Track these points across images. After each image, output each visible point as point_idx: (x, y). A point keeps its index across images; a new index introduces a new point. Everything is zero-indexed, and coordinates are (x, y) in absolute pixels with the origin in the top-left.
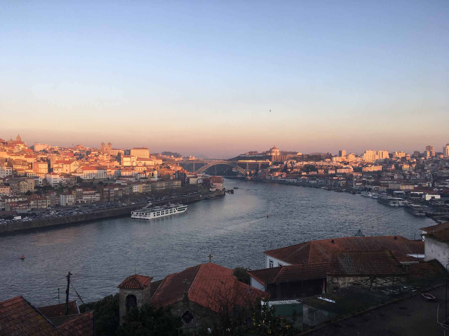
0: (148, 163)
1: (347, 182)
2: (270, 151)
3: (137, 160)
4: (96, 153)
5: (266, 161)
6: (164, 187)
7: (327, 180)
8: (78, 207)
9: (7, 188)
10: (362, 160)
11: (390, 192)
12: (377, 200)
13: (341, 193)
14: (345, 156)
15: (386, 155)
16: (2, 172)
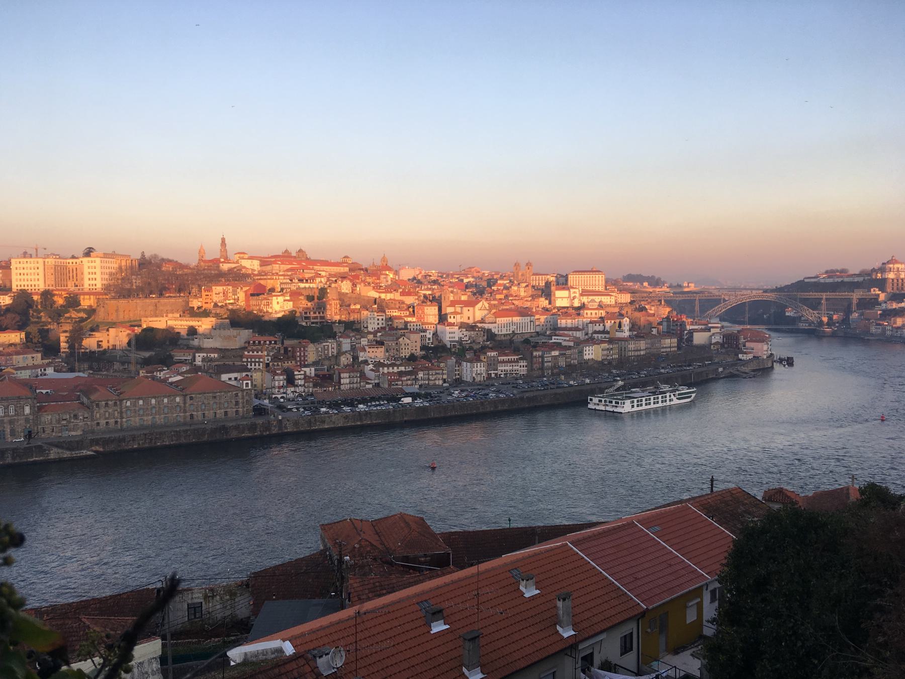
0: (606, 300)
3: (581, 295)
6: (643, 350)
8: (493, 385)
9: (380, 349)
16: (371, 321)
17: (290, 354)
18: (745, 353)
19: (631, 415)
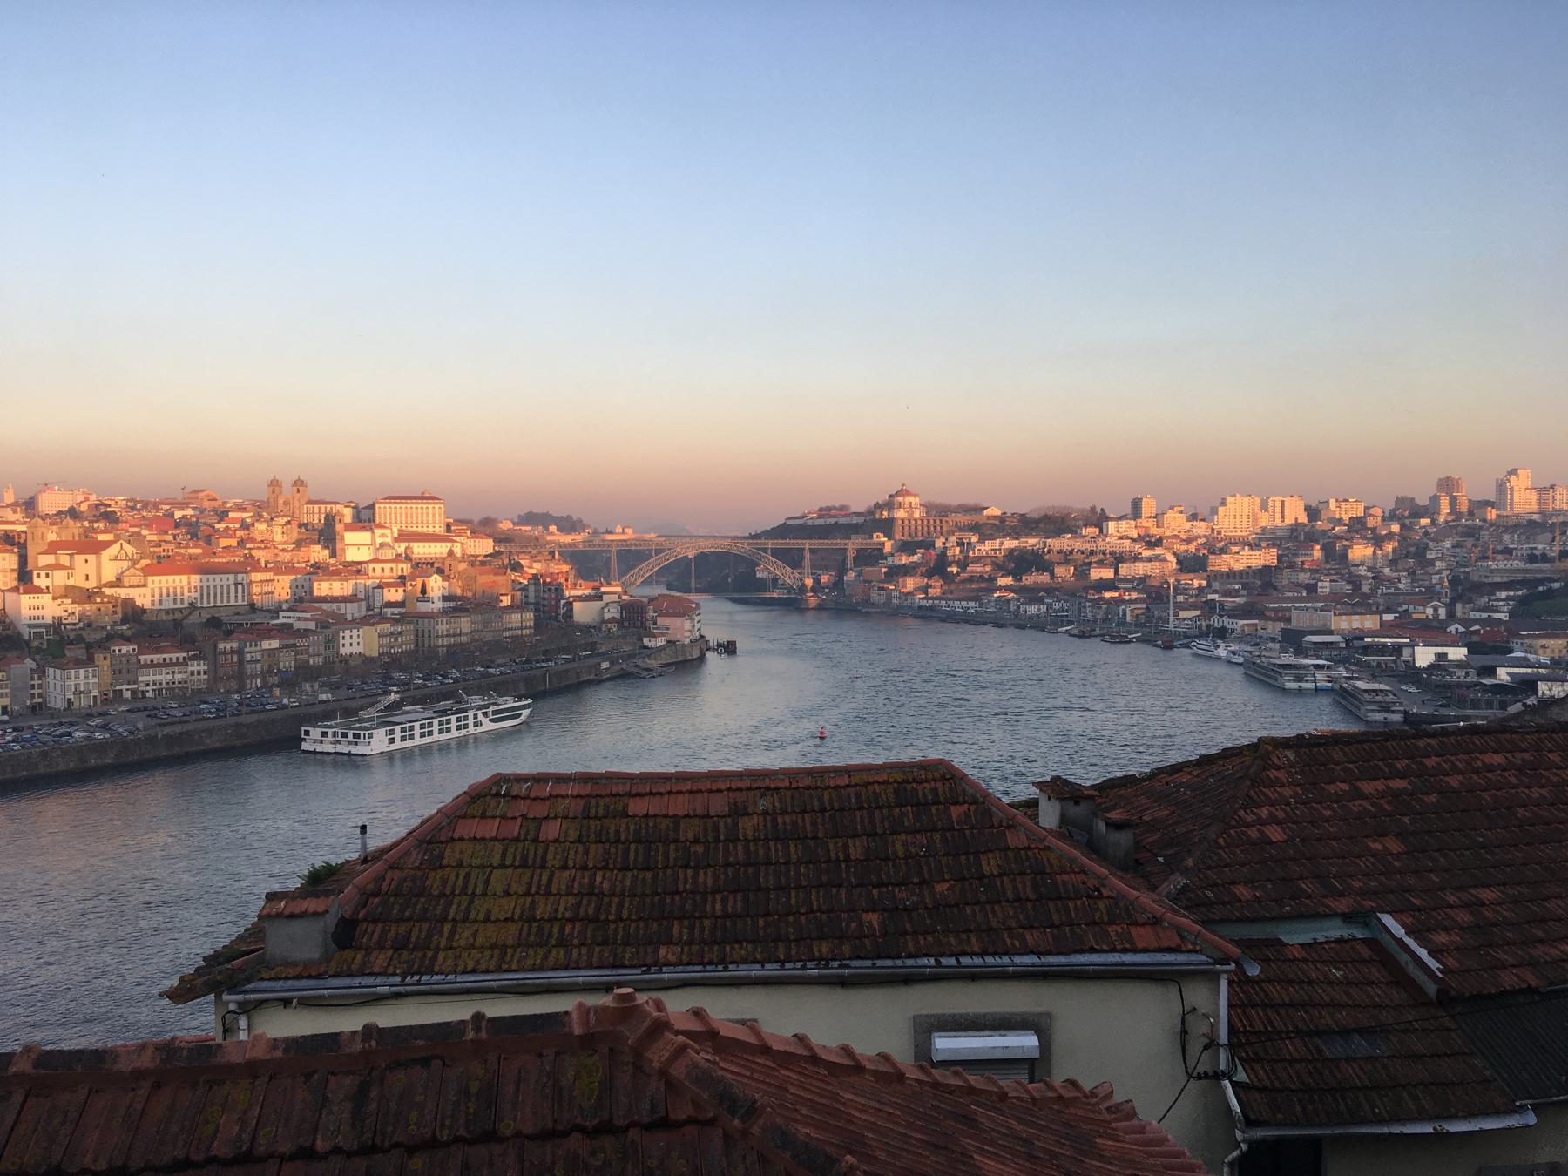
1: (1147, 608)
2: (890, 505)
4: (246, 516)
5: (872, 537)
7: (1080, 604)
10: (1213, 529)
11: (1293, 640)
12: (1242, 670)
13: (1123, 646)
14: (1151, 517)
15: (1295, 513)
18: (654, 636)
19: (389, 756)
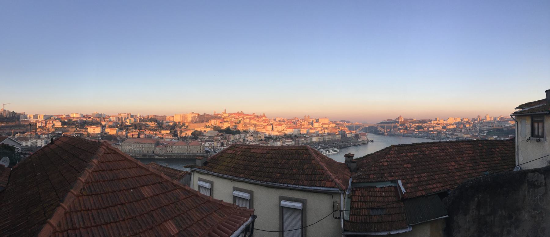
2: (398, 119)
17: (226, 138)
